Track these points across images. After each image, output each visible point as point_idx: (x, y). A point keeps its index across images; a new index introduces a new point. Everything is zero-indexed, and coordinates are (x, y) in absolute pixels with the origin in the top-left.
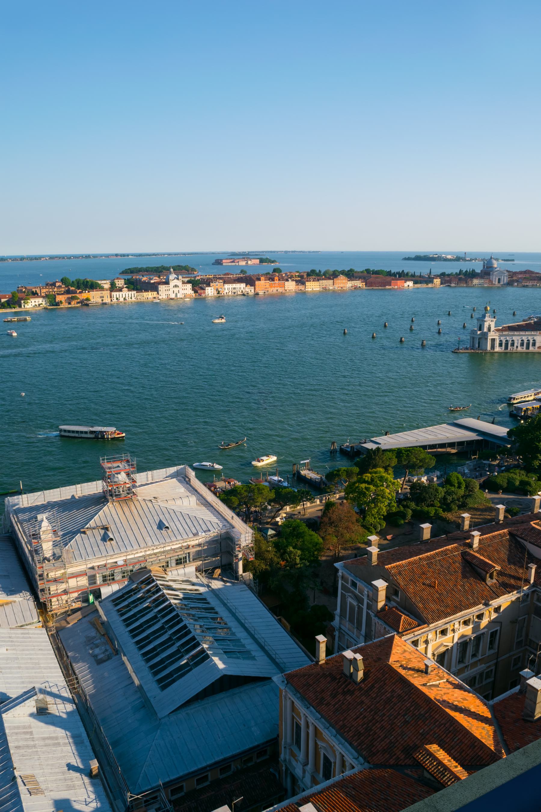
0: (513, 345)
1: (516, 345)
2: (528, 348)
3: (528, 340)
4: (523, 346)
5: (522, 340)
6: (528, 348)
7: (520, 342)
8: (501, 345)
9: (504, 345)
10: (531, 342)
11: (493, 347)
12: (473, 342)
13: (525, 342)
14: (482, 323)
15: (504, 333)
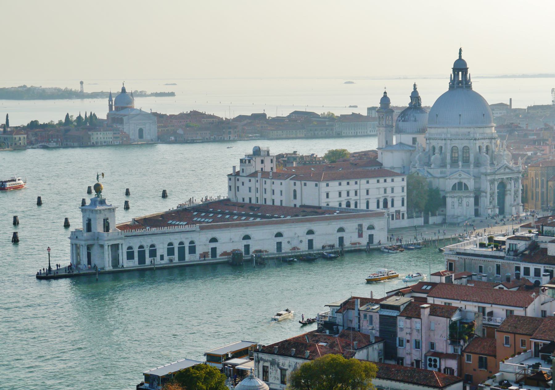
0: (153, 253)
1: (158, 254)
2: (182, 256)
3: (182, 243)
4: (174, 255)
5: (170, 244)
6: (182, 256)
7: (166, 246)
8: (130, 256)
9: (136, 255)
10: (187, 246)
11: (116, 261)
12: (78, 254)
13: (176, 246)
14: (92, 216)
15: (134, 232)
